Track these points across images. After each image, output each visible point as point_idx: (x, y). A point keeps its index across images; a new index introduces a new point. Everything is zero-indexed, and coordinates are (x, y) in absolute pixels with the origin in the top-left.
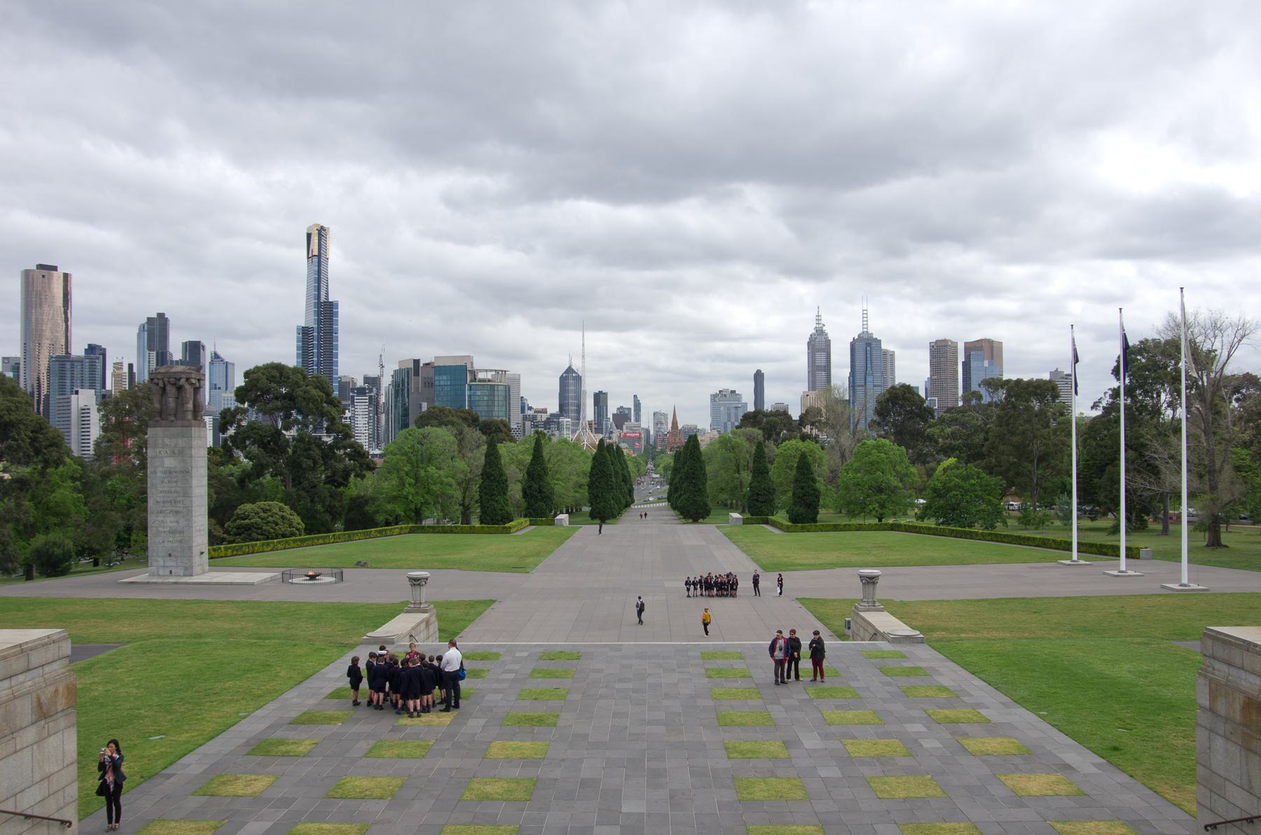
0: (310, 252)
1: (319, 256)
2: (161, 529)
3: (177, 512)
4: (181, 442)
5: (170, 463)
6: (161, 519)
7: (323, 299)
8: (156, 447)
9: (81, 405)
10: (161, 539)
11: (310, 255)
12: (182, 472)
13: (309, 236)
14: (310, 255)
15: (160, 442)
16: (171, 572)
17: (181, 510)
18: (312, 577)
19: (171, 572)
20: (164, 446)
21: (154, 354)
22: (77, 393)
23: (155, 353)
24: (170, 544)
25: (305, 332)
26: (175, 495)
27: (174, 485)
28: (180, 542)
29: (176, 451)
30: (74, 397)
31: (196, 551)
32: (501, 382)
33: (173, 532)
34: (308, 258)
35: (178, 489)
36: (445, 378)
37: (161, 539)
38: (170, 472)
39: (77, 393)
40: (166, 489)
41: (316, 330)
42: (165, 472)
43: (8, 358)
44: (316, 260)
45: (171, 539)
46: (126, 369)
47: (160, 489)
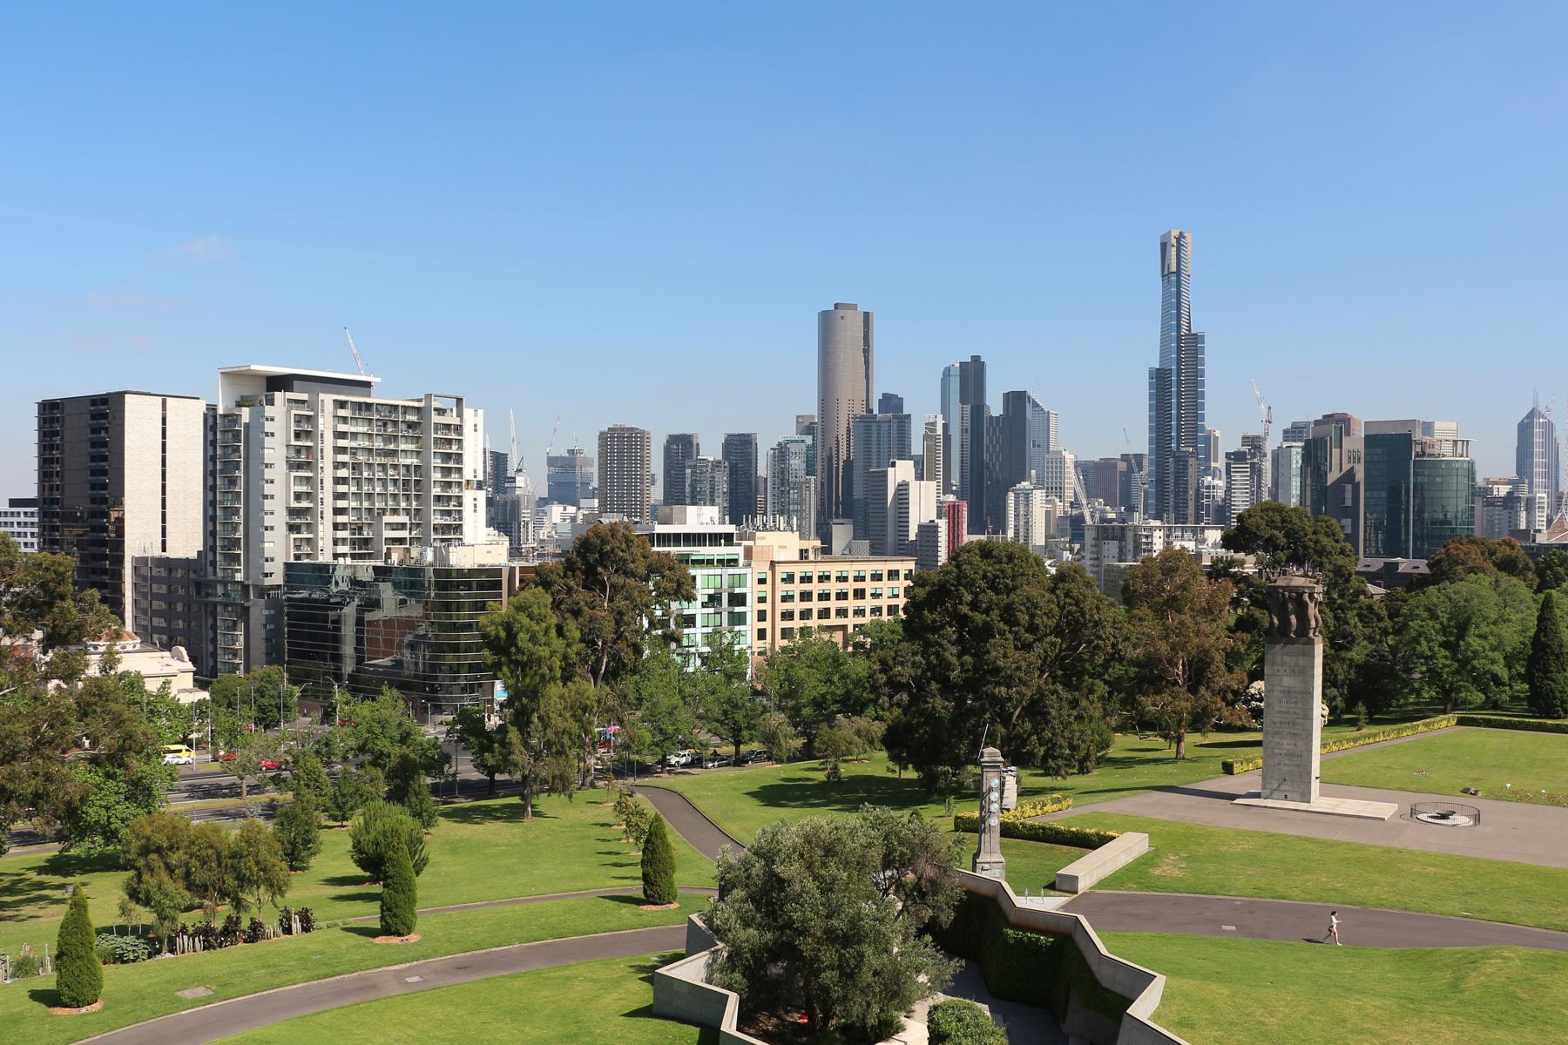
0: (1166, 268)
1: (1178, 273)
2: (1276, 751)
3: (1294, 734)
4: (1302, 661)
5: (1288, 682)
6: (1277, 740)
7: (1184, 331)
8: (1274, 664)
9: (899, 480)
10: (1276, 761)
11: (1166, 272)
12: (1302, 693)
13: (1164, 247)
14: (1166, 272)
15: (1278, 659)
16: (1286, 796)
17: (1300, 732)
18: (1444, 817)
19: (1286, 796)
20: (1284, 664)
21: (968, 408)
22: (893, 465)
23: (969, 406)
24: (1286, 768)
25: (1160, 378)
26: (1294, 716)
27: (1293, 705)
28: (1298, 766)
29: (1296, 669)
30: (890, 470)
31: (1313, 778)
32: (1462, 456)
33: (1290, 755)
34: (1163, 276)
35: (1297, 710)
36: (1379, 451)
37: (1276, 761)
38: (1288, 692)
39: (893, 465)
40: (1285, 709)
41: (1174, 372)
42: (1284, 692)
43: (802, 417)
44: (1174, 278)
45: (1287, 762)
46: (940, 431)
47: (1277, 708)
